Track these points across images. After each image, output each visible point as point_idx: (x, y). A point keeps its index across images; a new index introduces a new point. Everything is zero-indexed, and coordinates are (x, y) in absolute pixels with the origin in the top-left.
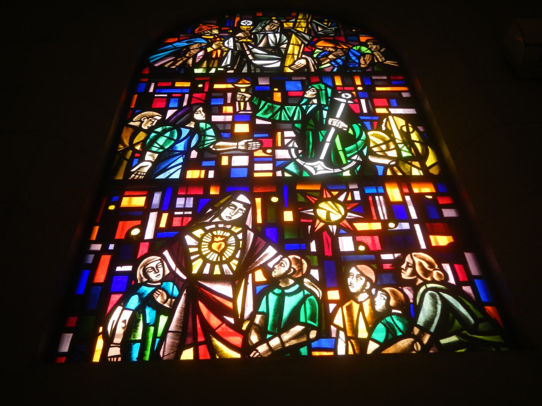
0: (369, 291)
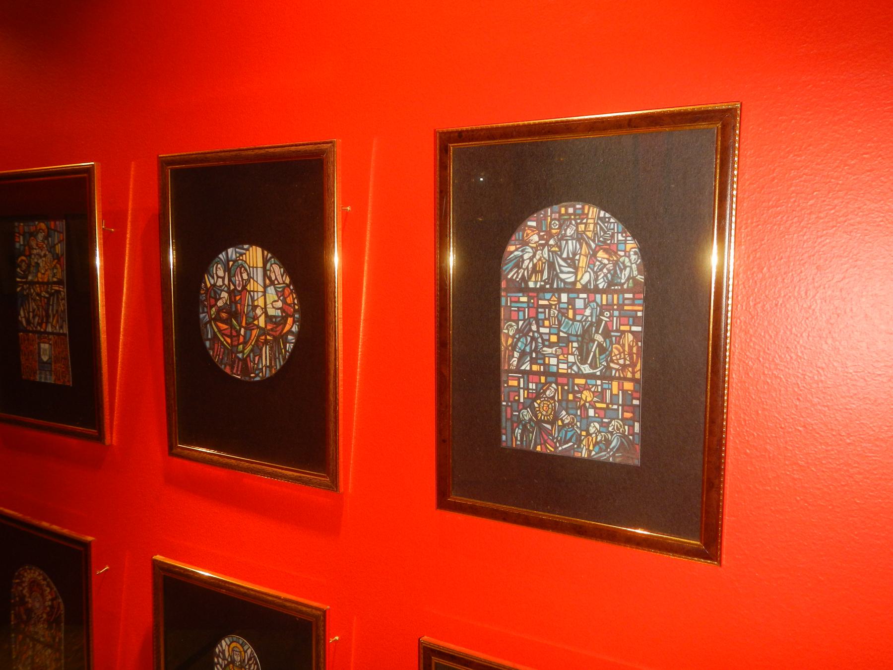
0: (596, 434)
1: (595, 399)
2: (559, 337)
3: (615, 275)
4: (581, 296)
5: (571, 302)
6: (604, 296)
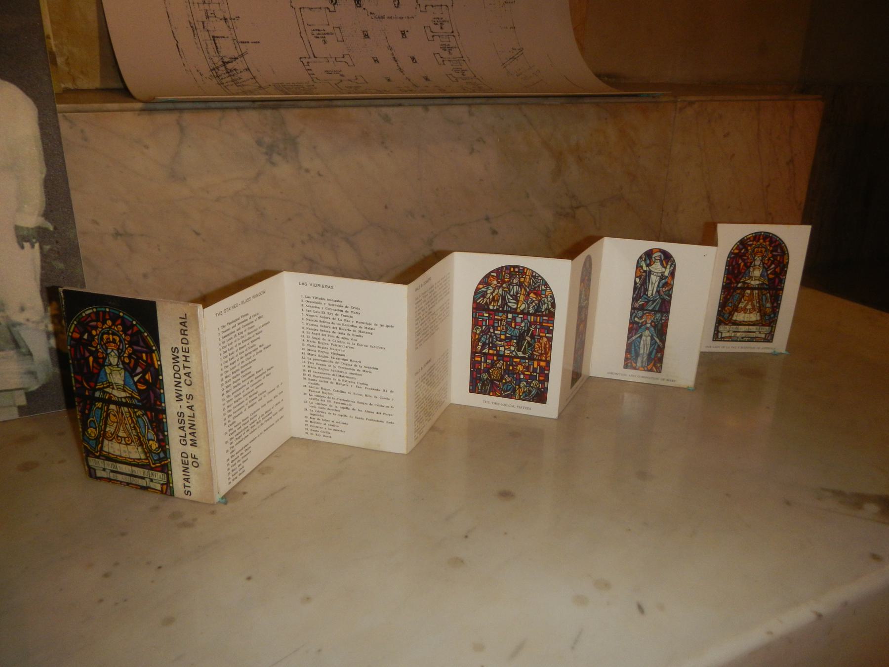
1: (524, 370)
2: (506, 336)
3: (539, 307)
4: (520, 316)
5: (514, 319)
6: (532, 317)
